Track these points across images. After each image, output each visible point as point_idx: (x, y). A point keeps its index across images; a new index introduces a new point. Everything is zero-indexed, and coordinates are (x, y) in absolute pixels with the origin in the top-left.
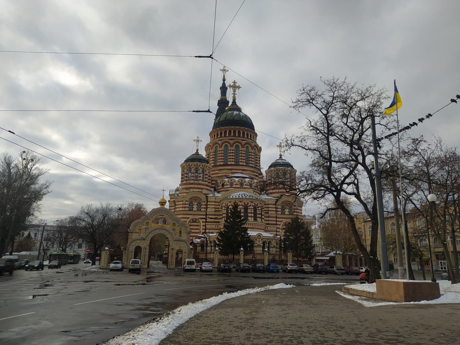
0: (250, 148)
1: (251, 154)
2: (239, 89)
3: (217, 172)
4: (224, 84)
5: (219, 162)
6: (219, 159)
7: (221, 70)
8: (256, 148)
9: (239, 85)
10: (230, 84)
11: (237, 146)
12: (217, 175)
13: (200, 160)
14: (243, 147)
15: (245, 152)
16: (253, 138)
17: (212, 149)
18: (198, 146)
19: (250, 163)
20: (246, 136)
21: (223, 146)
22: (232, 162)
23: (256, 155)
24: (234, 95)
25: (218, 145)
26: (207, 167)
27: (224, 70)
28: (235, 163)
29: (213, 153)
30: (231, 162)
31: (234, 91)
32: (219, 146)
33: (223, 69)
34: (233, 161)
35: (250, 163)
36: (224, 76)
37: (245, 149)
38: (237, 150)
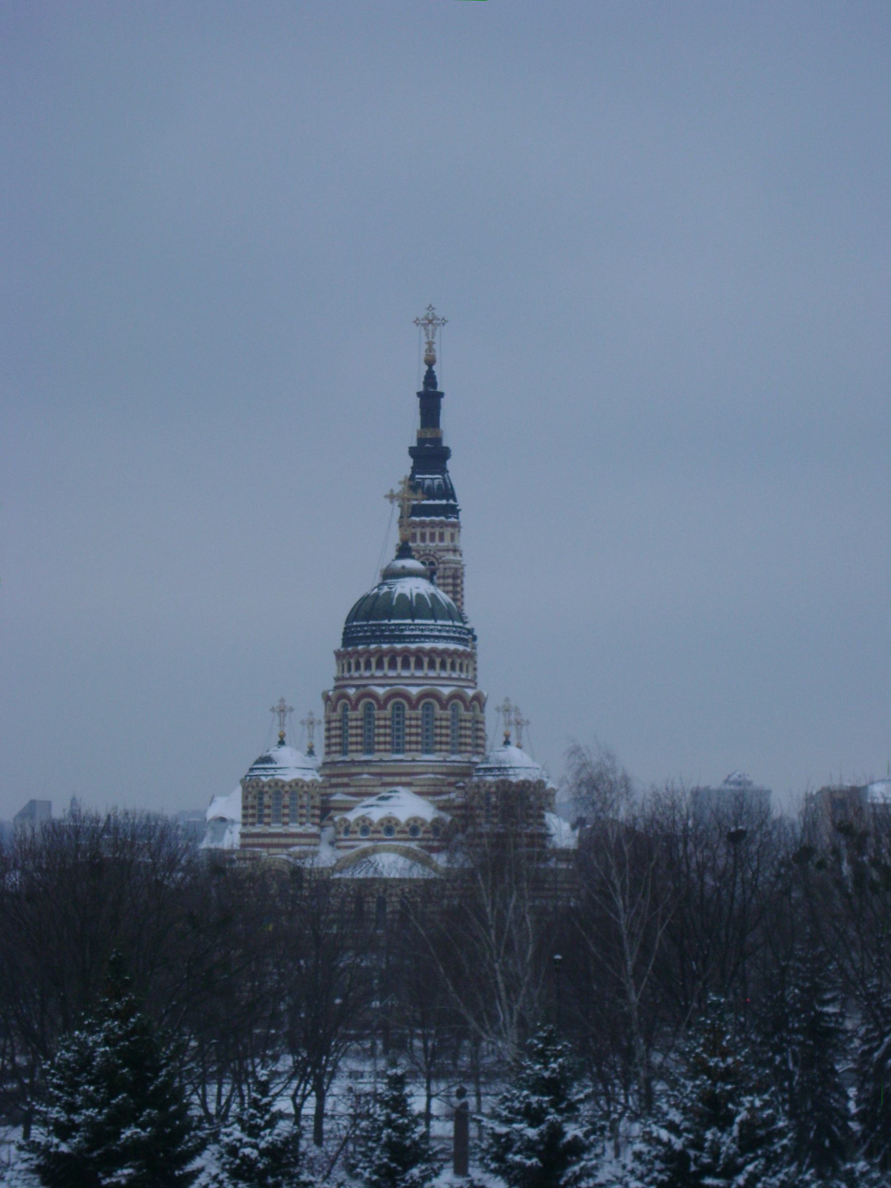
1: (438, 723)
3: (345, 780)
4: (430, 379)
6: (351, 743)
7: (416, 322)
10: (392, 491)
11: (398, 707)
12: (346, 790)
14: (413, 707)
15: (420, 723)
17: (334, 710)
18: (282, 724)
23: (461, 721)
26: (302, 787)
27: (430, 322)
29: (338, 724)
33: (426, 318)
36: (430, 344)
37: (419, 712)
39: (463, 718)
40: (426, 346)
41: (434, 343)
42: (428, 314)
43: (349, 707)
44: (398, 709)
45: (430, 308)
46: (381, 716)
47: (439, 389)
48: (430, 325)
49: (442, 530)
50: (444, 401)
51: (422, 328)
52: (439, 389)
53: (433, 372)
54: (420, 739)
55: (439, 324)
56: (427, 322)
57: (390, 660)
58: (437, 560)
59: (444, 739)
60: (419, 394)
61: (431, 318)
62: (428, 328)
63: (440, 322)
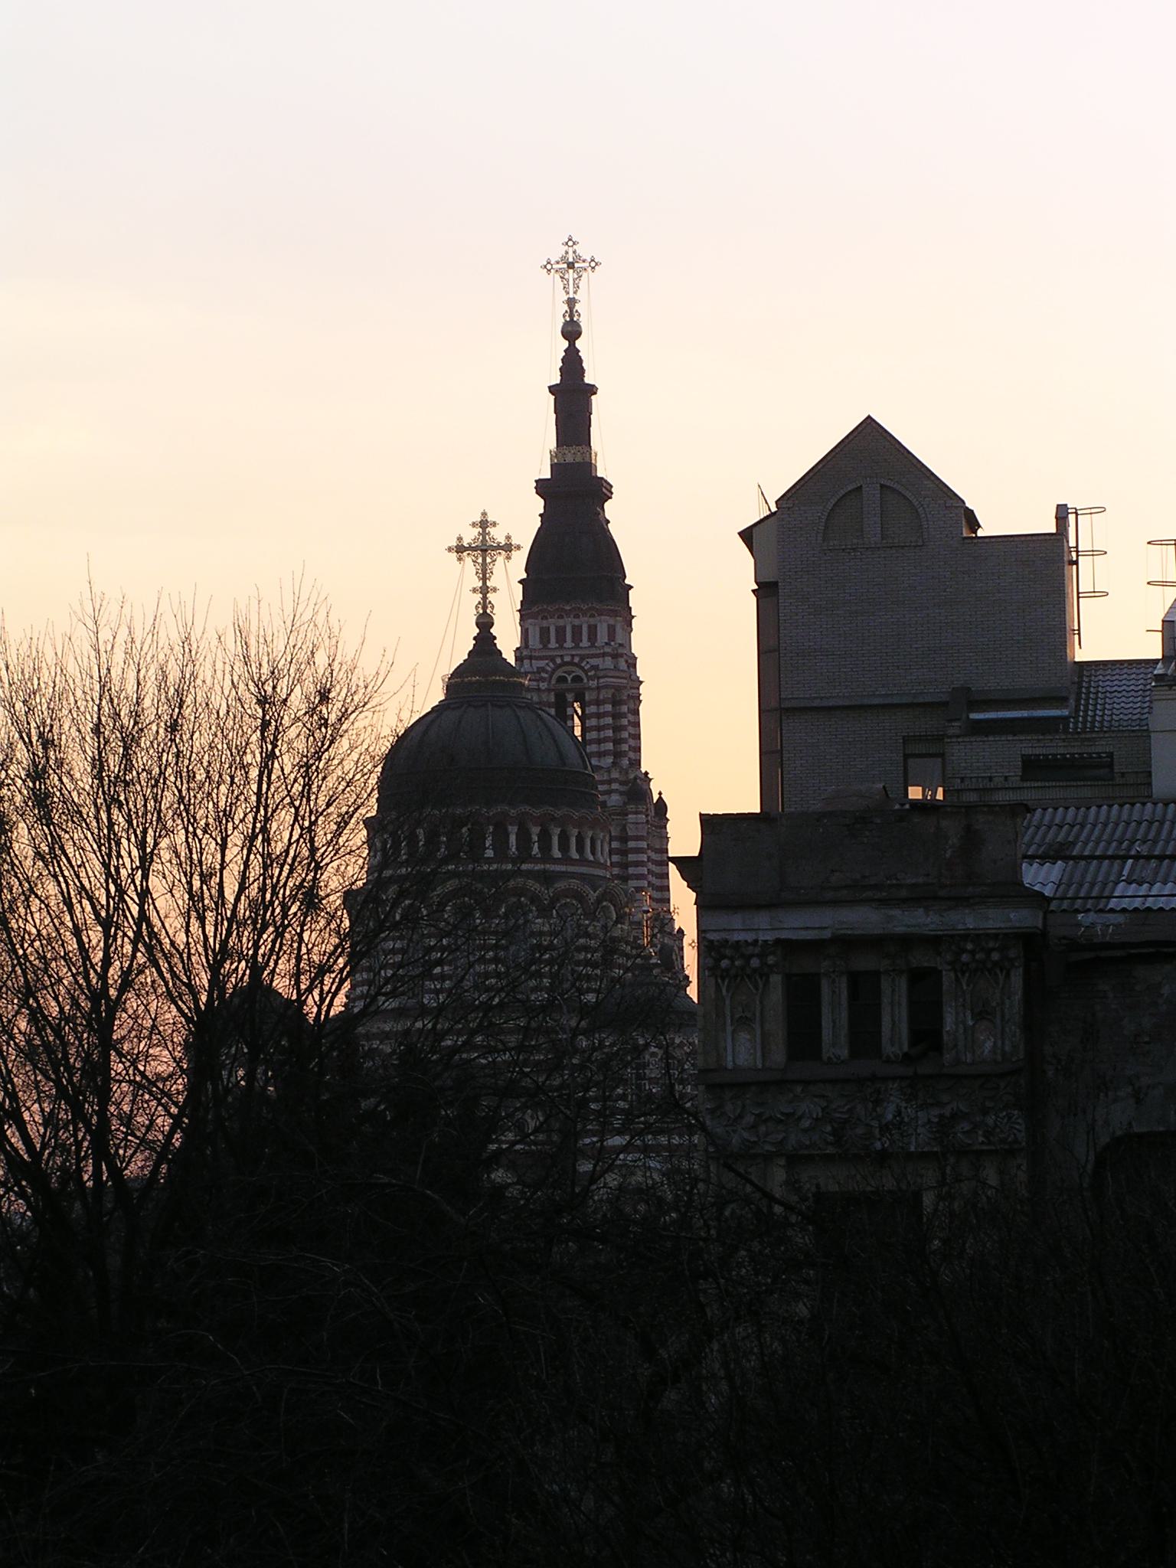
2: (508, 558)
4: (572, 364)
7: (547, 267)
16: (564, 847)
24: (485, 598)
27: (571, 266)
31: (484, 574)
33: (564, 259)
36: (571, 303)
40: (566, 307)
42: (567, 253)
45: (570, 242)
48: (571, 271)
49: (592, 621)
51: (557, 276)
58: (586, 672)
60: (552, 389)
61: (571, 260)
62: (566, 277)
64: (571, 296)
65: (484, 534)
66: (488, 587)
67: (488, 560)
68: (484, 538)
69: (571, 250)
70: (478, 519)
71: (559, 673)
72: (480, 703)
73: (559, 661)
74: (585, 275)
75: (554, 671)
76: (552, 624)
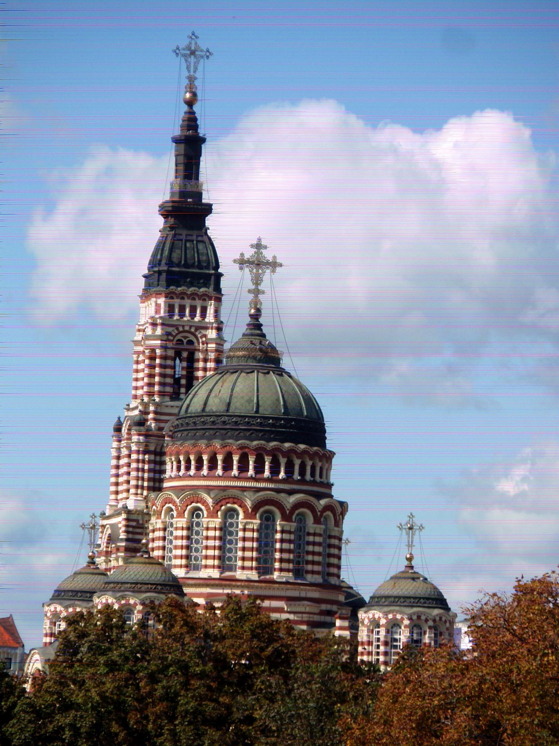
0: (310, 519)
1: (311, 539)
2: (273, 271)
5: (206, 567)
7: (177, 52)
8: (329, 513)
9: (274, 257)
13: (159, 587)
16: (321, 476)
19: (307, 572)
20: (297, 476)
21: (219, 513)
22: (249, 572)
23: (330, 537)
24: (256, 296)
25: (203, 508)
27: (193, 53)
28: (260, 574)
30: (246, 572)
31: (257, 280)
32: (205, 513)
33: (188, 48)
34: (251, 568)
35: (307, 572)
36: (191, 79)
38: (267, 527)
39: (333, 534)
40: (186, 82)
41: (196, 78)
42: (190, 43)
43: (175, 513)
44: (267, 519)
46: (247, 527)
47: (201, 132)
48: (192, 57)
50: (205, 149)
51: (183, 59)
52: (201, 135)
53: (194, 113)
54: (292, 556)
55: (202, 57)
56: (188, 52)
57: (256, 459)
59: (317, 558)
61: (193, 48)
62: (189, 60)
63: (204, 54)
64: (192, 73)
65: (258, 253)
66: (259, 290)
67: (260, 271)
68: (258, 255)
69: (193, 42)
70: (255, 242)
71: (179, 337)
72: (266, 371)
73: (181, 329)
74: (202, 61)
75: (177, 334)
76: (177, 302)
